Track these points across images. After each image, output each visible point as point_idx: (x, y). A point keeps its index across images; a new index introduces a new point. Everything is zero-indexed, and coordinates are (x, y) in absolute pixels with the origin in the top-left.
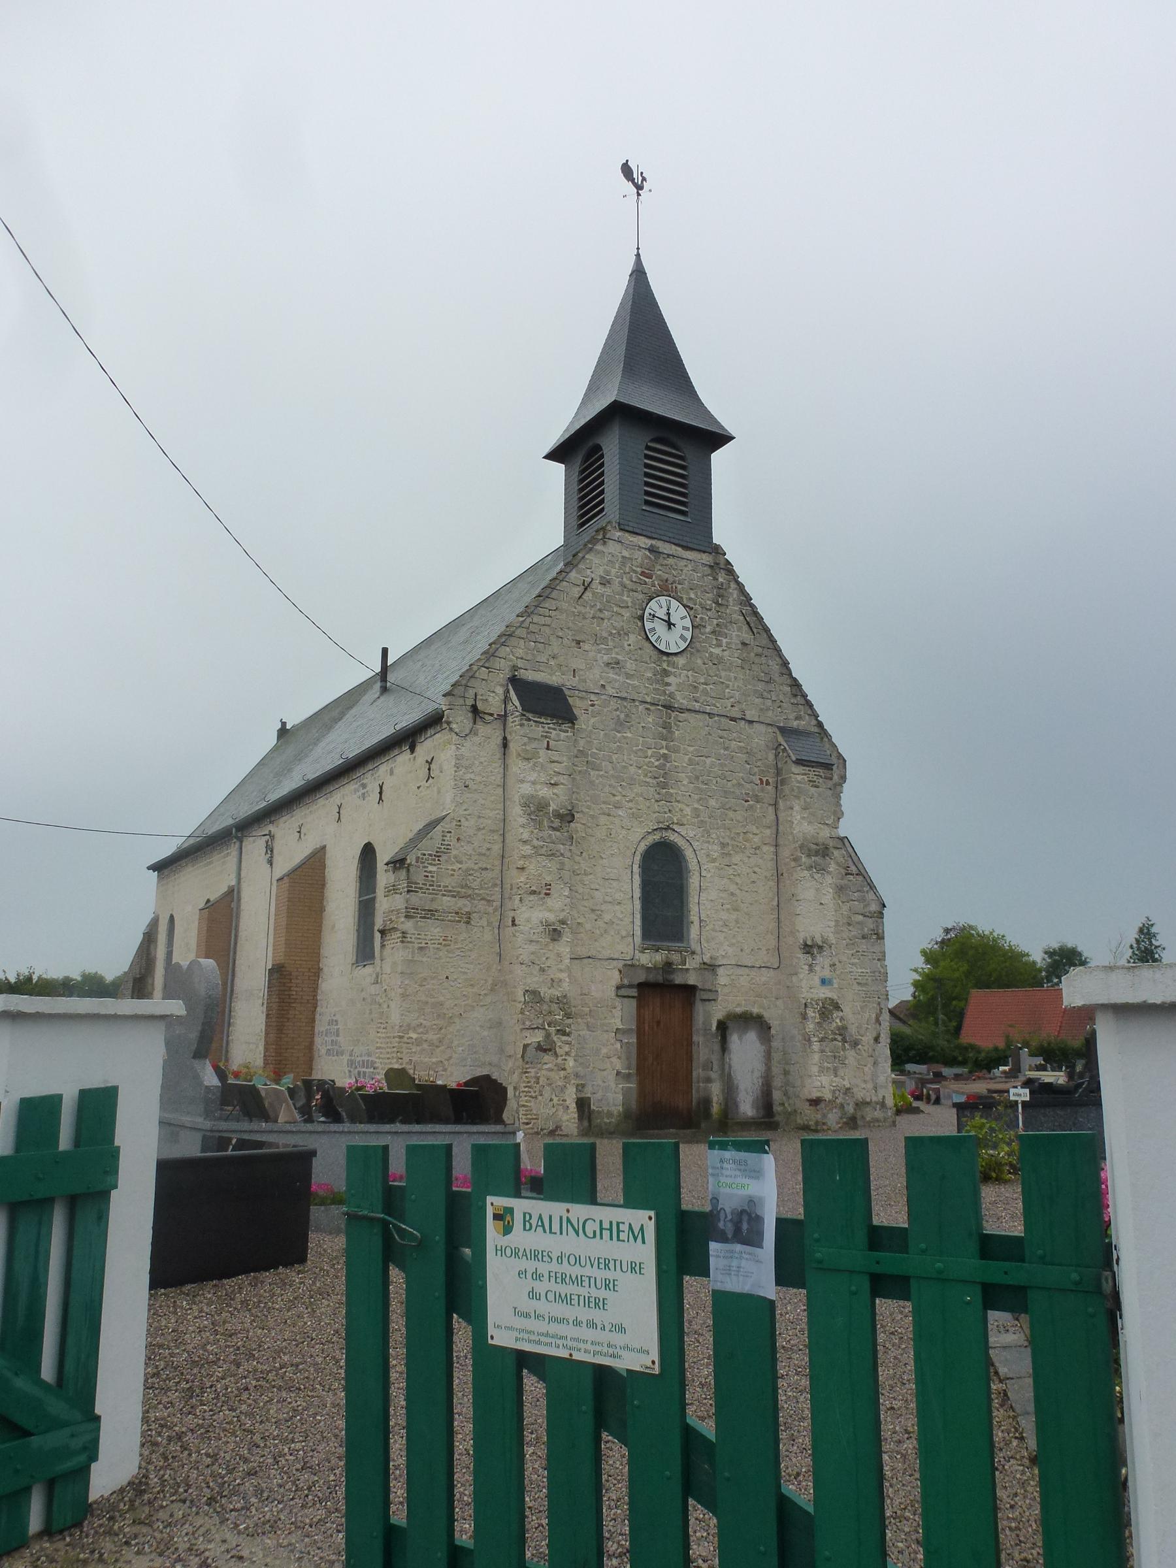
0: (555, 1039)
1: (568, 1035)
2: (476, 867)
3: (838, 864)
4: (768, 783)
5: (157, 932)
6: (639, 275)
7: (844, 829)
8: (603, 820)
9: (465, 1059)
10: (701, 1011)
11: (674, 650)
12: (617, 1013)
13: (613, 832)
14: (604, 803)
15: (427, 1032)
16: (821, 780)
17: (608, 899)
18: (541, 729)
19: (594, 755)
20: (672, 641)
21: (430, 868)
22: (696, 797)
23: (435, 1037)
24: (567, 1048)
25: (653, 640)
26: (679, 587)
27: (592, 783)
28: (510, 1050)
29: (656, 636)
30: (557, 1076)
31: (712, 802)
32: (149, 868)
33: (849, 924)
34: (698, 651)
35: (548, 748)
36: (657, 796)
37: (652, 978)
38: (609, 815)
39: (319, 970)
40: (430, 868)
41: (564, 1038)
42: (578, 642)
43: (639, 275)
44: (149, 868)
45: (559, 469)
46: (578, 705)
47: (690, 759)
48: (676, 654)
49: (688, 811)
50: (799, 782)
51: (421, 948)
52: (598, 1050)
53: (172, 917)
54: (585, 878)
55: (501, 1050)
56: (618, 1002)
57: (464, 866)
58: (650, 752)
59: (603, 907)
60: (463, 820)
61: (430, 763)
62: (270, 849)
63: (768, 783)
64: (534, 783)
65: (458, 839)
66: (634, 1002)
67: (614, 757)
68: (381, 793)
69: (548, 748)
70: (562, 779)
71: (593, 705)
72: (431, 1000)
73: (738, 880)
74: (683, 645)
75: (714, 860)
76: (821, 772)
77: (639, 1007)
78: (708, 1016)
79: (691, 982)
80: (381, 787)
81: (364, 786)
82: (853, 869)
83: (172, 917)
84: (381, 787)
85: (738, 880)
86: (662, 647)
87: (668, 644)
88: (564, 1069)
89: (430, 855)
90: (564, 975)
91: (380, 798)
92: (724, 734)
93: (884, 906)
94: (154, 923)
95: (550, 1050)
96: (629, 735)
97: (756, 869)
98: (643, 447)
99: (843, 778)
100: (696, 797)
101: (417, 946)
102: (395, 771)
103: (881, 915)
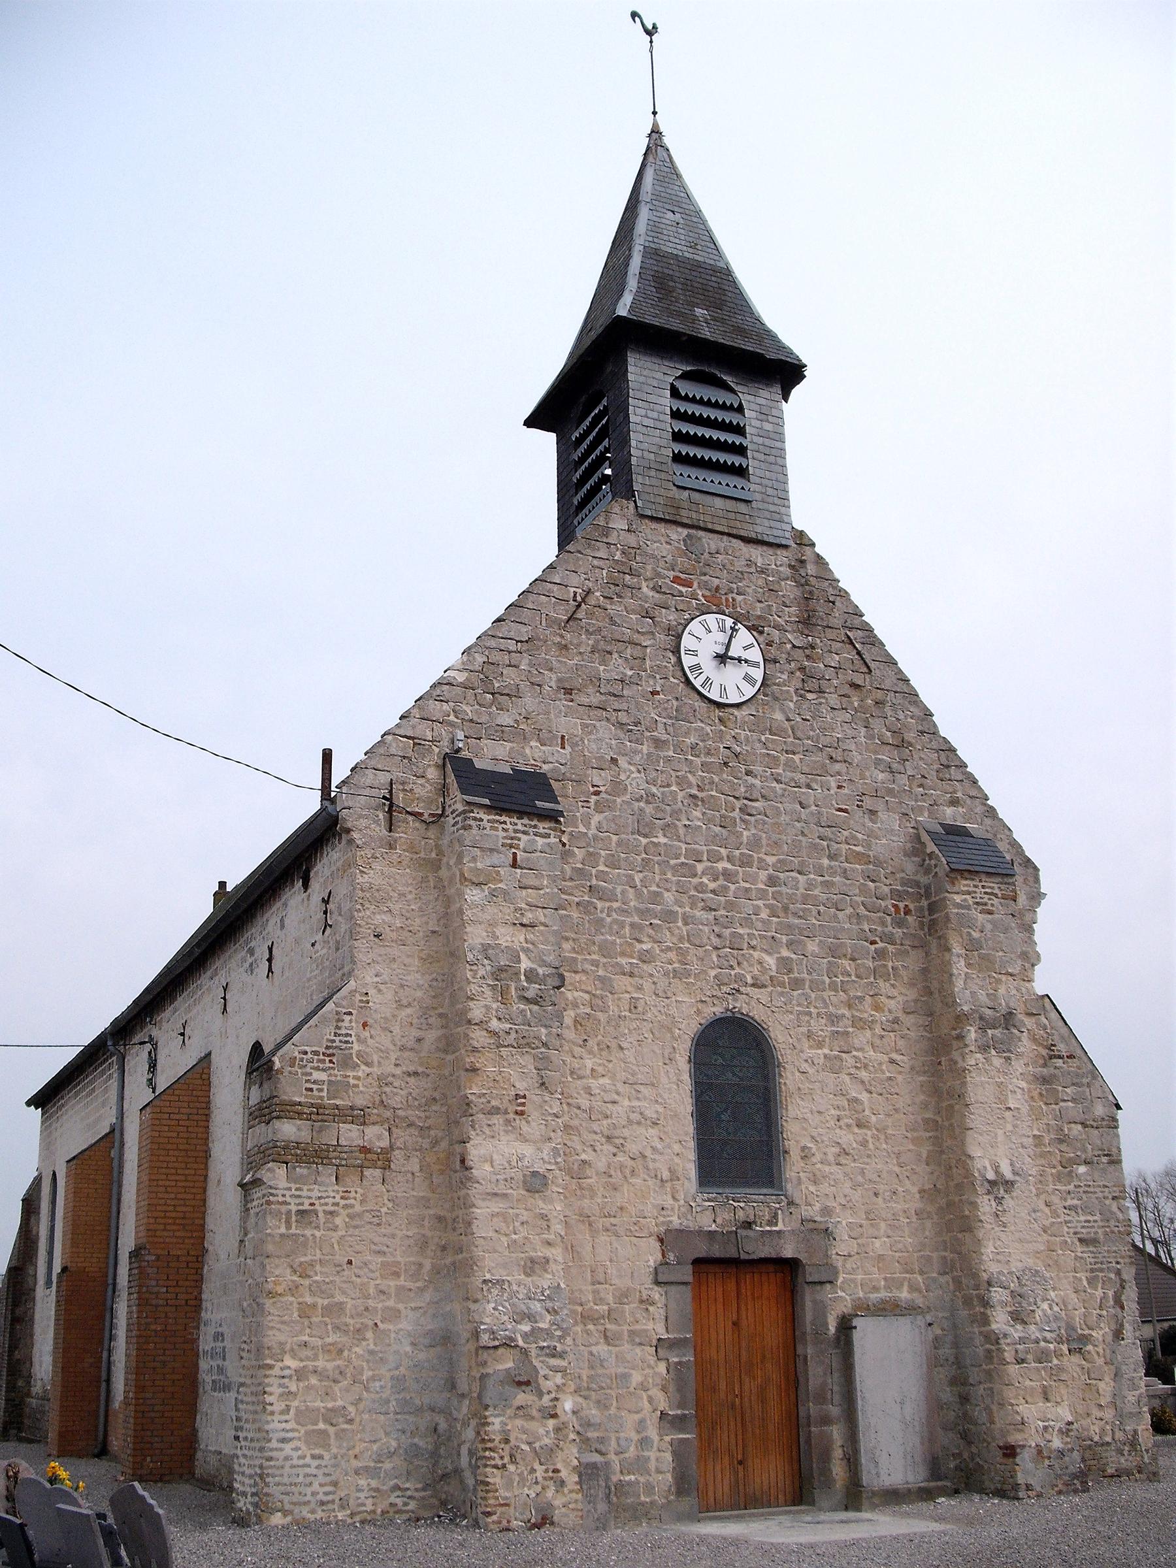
0: (535, 1362)
1: (562, 1355)
2: (398, 1071)
3: (1034, 1040)
4: (907, 912)
5: (39, 1198)
6: (655, 132)
7: (1043, 982)
8: (622, 982)
9: (388, 1401)
10: (808, 1304)
11: (734, 699)
12: (658, 1311)
13: (640, 1004)
14: (623, 954)
15: (315, 1358)
16: (996, 901)
17: (635, 1117)
18: (501, 834)
19: (601, 876)
20: (732, 685)
21: (317, 1075)
22: (784, 939)
23: (330, 1366)
24: (559, 1379)
25: (697, 683)
26: (739, 598)
27: (599, 922)
28: (463, 1386)
29: (702, 678)
30: (544, 1431)
31: (812, 947)
32: (29, 1103)
33: (1061, 1141)
34: (776, 699)
35: (514, 865)
36: (716, 941)
37: (717, 1251)
38: (631, 975)
39: (204, 1251)
40: (317, 1075)
41: (553, 1362)
42: (568, 691)
43: (655, 132)
44: (29, 1103)
45: (548, 440)
46: (568, 798)
47: (770, 877)
48: (738, 706)
49: (771, 961)
50: (959, 906)
51: (301, 1213)
52: (626, 1377)
53: (54, 1174)
54: (593, 1083)
55: (452, 1385)
56: (657, 1294)
57: (376, 1070)
58: (700, 867)
59: (626, 1132)
60: (372, 992)
61: (326, 902)
62: (153, 1066)
63: (907, 912)
64: (492, 924)
65: (365, 1025)
66: (687, 1292)
67: (638, 878)
68: (270, 960)
69: (514, 865)
70: (540, 915)
71: (597, 793)
72: (321, 1302)
73: (864, 1074)
74: (749, 691)
75: (820, 1045)
76: (994, 885)
77: (697, 1298)
78: (821, 1310)
79: (788, 1253)
80: (270, 950)
81: (251, 952)
82: (1062, 1048)
83: (54, 1174)
84: (270, 950)
85: (864, 1074)
86: (714, 695)
87: (723, 689)
88: (554, 1416)
89: (316, 1053)
90: (556, 1253)
91: (270, 970)
92: (828, 832)
93: (1118, 1107)
94: (37, 1181)
95: (528, 1383)
96: (663, 840)
97: (895, 1056)
98: (665, 376)
99: (1037, 897)
100: (784, 939)
101: (294, 1208)
102: (287, 921)
103: (1113, 1124)
